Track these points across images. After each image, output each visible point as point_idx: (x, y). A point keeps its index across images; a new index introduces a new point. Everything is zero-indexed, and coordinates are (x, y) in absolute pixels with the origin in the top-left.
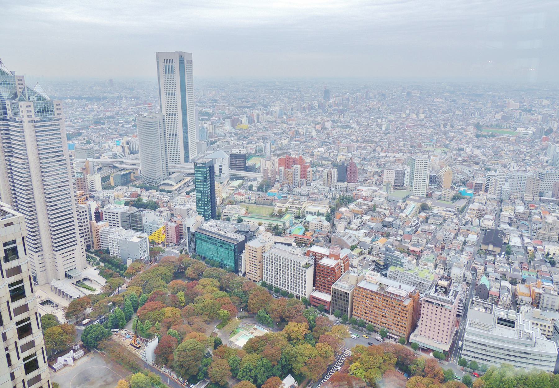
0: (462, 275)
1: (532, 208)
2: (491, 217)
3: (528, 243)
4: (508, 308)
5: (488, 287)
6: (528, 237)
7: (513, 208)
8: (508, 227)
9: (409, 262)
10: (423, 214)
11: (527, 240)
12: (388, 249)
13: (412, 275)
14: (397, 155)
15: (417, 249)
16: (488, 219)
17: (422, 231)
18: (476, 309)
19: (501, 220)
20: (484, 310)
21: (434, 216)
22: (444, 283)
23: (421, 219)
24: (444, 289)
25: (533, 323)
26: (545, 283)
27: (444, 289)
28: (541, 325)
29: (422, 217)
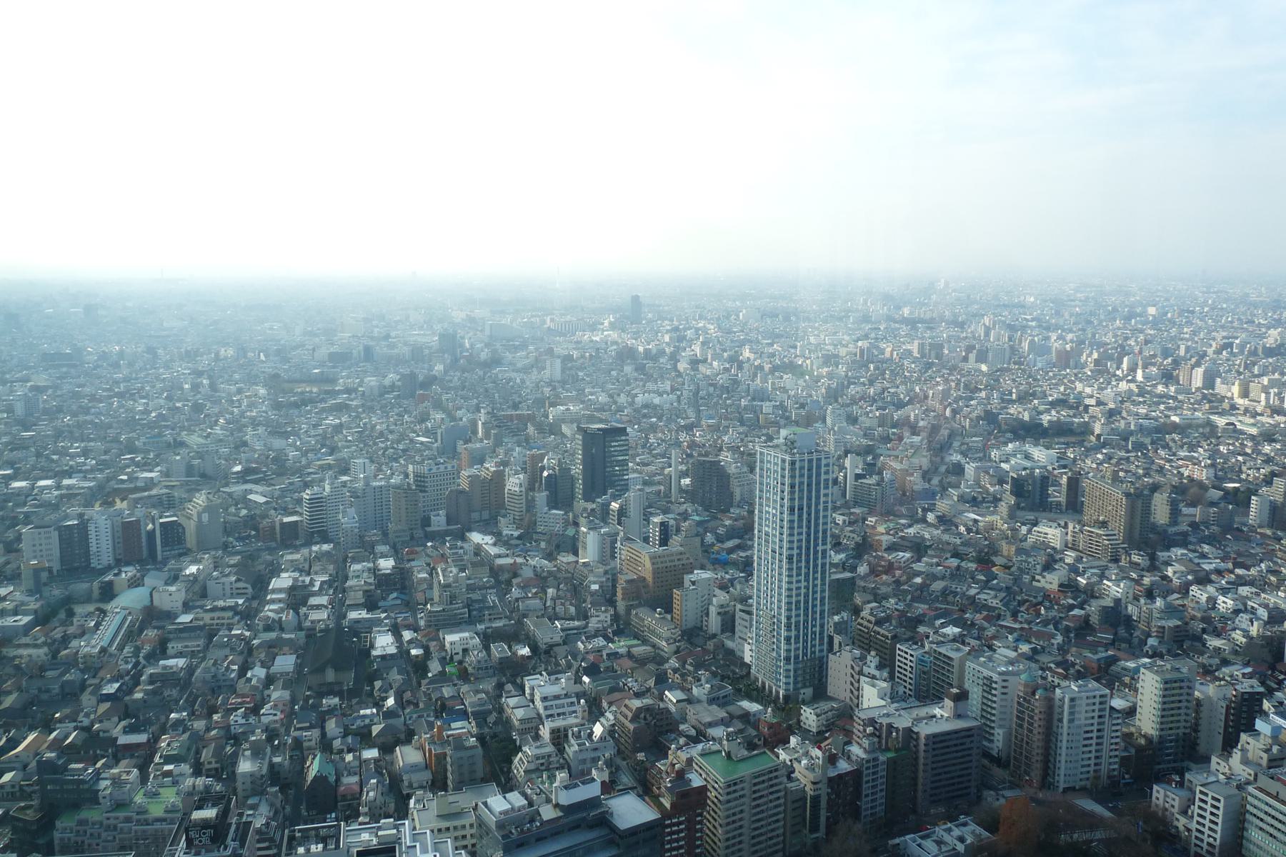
0: (265, 771)
1: (411, 557)
2: (323, 600)
3: (410, 642)
4: (375, 817)
5: (332, 779)
6: (408, 627)
7: (371, 565)
8: (363, 614)
9: (116, 781)
10: (151, 633)
11: (407, 635)
12: (44, 767)
13: (128, 820)
14: (66, 482)
15: (142, 738)
16: (318, 607)
17: (151, 683)
18: (301, 850)
19: (348, 602)
20: (320, 846)
21: (181, 631)
22: (209, 813)
23: (147, 648)
24: (210, 832)
25: (440, 830)
26: (453, 725)
27: (210, 832)
28: (455, 828)
29: (149, 641)
